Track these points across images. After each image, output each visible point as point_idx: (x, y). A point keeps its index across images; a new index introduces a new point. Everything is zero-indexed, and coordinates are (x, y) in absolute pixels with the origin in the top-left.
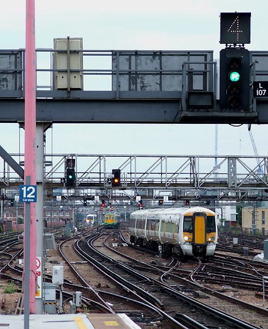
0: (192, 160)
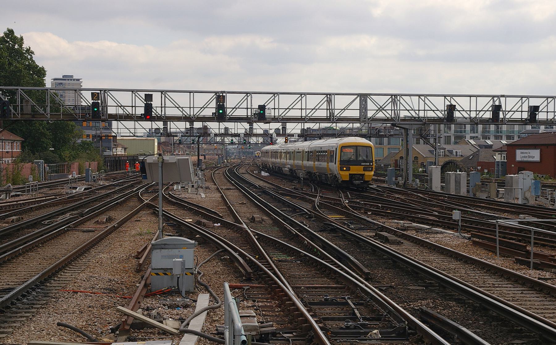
0: (329, 97)
